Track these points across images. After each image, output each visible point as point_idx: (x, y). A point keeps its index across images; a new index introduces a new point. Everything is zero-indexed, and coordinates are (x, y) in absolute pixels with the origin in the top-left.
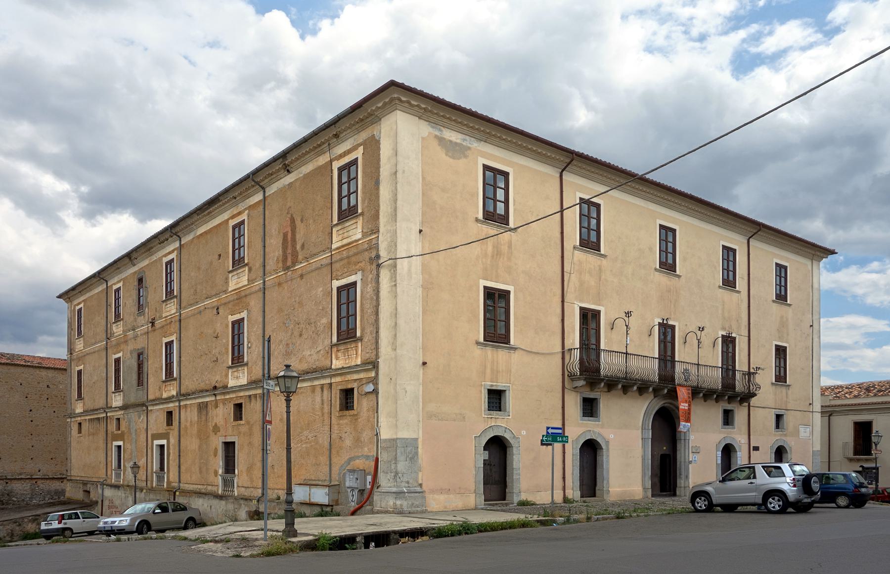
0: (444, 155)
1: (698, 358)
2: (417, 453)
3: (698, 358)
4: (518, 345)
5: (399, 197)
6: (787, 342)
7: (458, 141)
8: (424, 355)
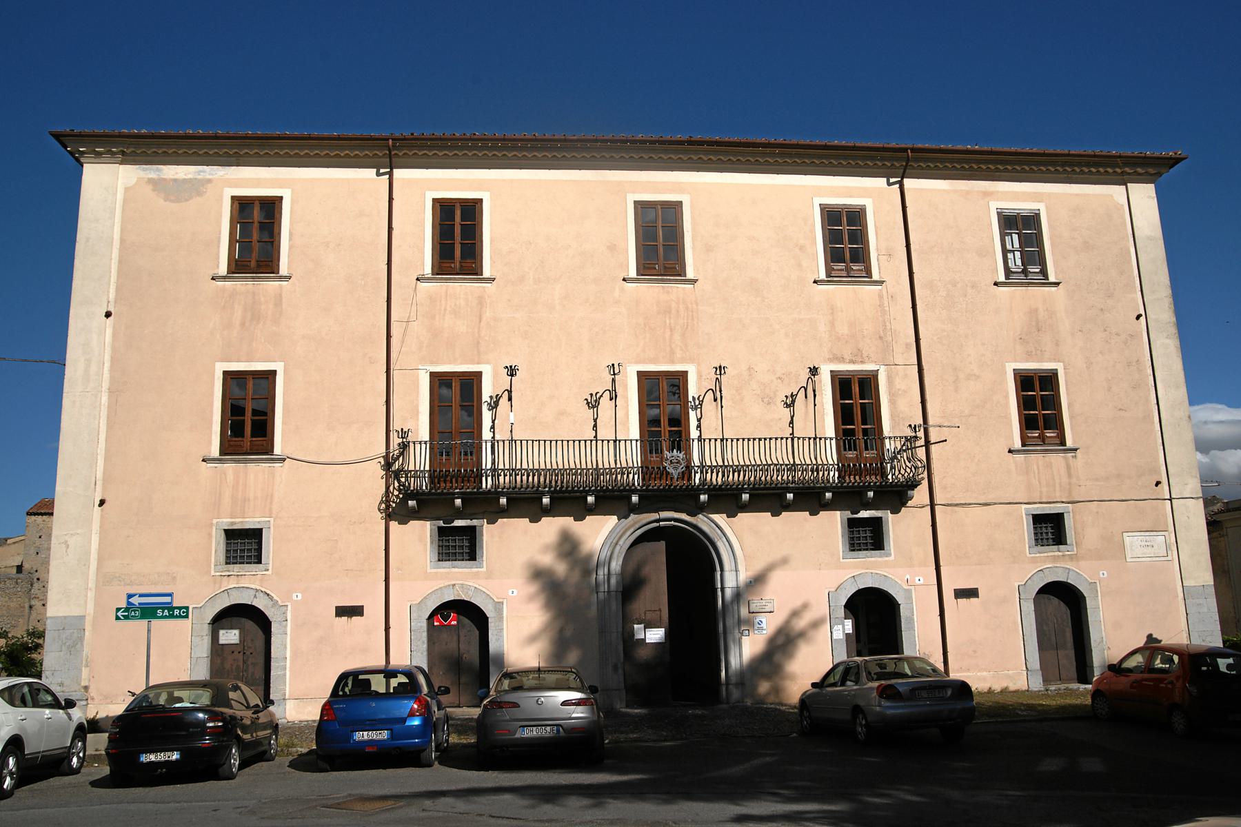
0: (161, 201)
1: (756, 416)
2: (81, 639)
3: (756, 416)
4: (288, 453)
5: (423, 789)
6: (1055, 360)
7: (190, 176)
8: (104, 488)
